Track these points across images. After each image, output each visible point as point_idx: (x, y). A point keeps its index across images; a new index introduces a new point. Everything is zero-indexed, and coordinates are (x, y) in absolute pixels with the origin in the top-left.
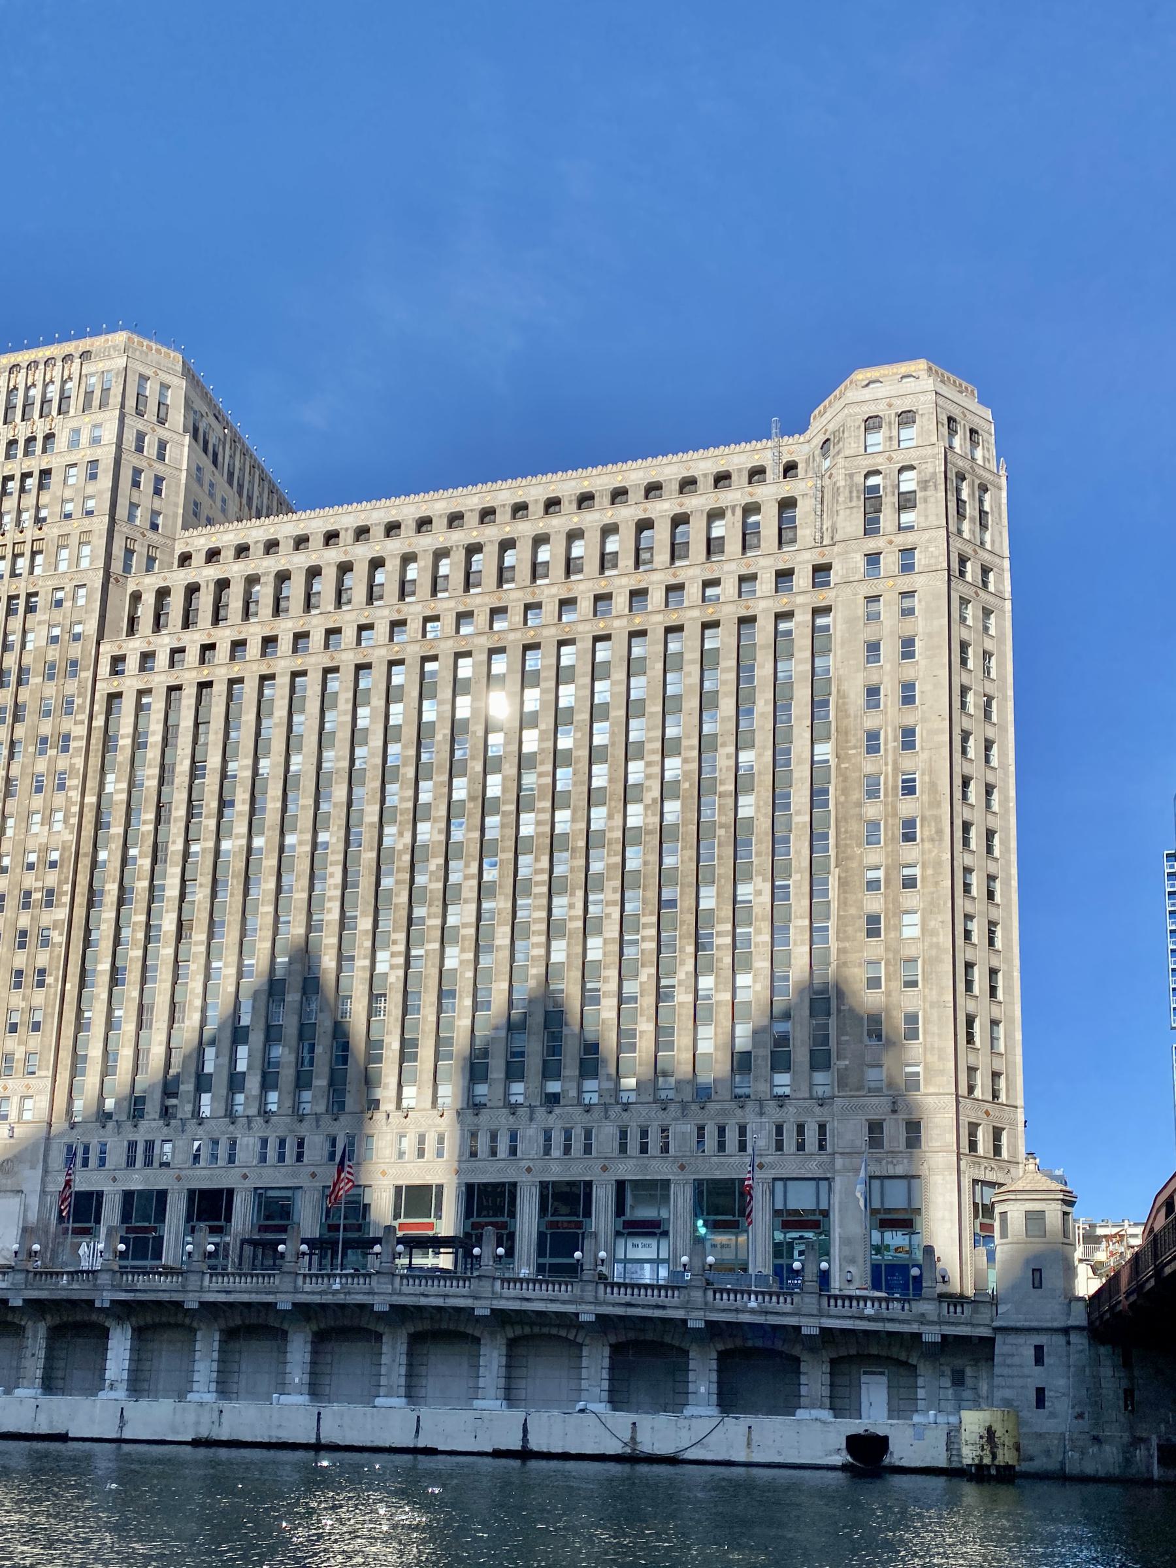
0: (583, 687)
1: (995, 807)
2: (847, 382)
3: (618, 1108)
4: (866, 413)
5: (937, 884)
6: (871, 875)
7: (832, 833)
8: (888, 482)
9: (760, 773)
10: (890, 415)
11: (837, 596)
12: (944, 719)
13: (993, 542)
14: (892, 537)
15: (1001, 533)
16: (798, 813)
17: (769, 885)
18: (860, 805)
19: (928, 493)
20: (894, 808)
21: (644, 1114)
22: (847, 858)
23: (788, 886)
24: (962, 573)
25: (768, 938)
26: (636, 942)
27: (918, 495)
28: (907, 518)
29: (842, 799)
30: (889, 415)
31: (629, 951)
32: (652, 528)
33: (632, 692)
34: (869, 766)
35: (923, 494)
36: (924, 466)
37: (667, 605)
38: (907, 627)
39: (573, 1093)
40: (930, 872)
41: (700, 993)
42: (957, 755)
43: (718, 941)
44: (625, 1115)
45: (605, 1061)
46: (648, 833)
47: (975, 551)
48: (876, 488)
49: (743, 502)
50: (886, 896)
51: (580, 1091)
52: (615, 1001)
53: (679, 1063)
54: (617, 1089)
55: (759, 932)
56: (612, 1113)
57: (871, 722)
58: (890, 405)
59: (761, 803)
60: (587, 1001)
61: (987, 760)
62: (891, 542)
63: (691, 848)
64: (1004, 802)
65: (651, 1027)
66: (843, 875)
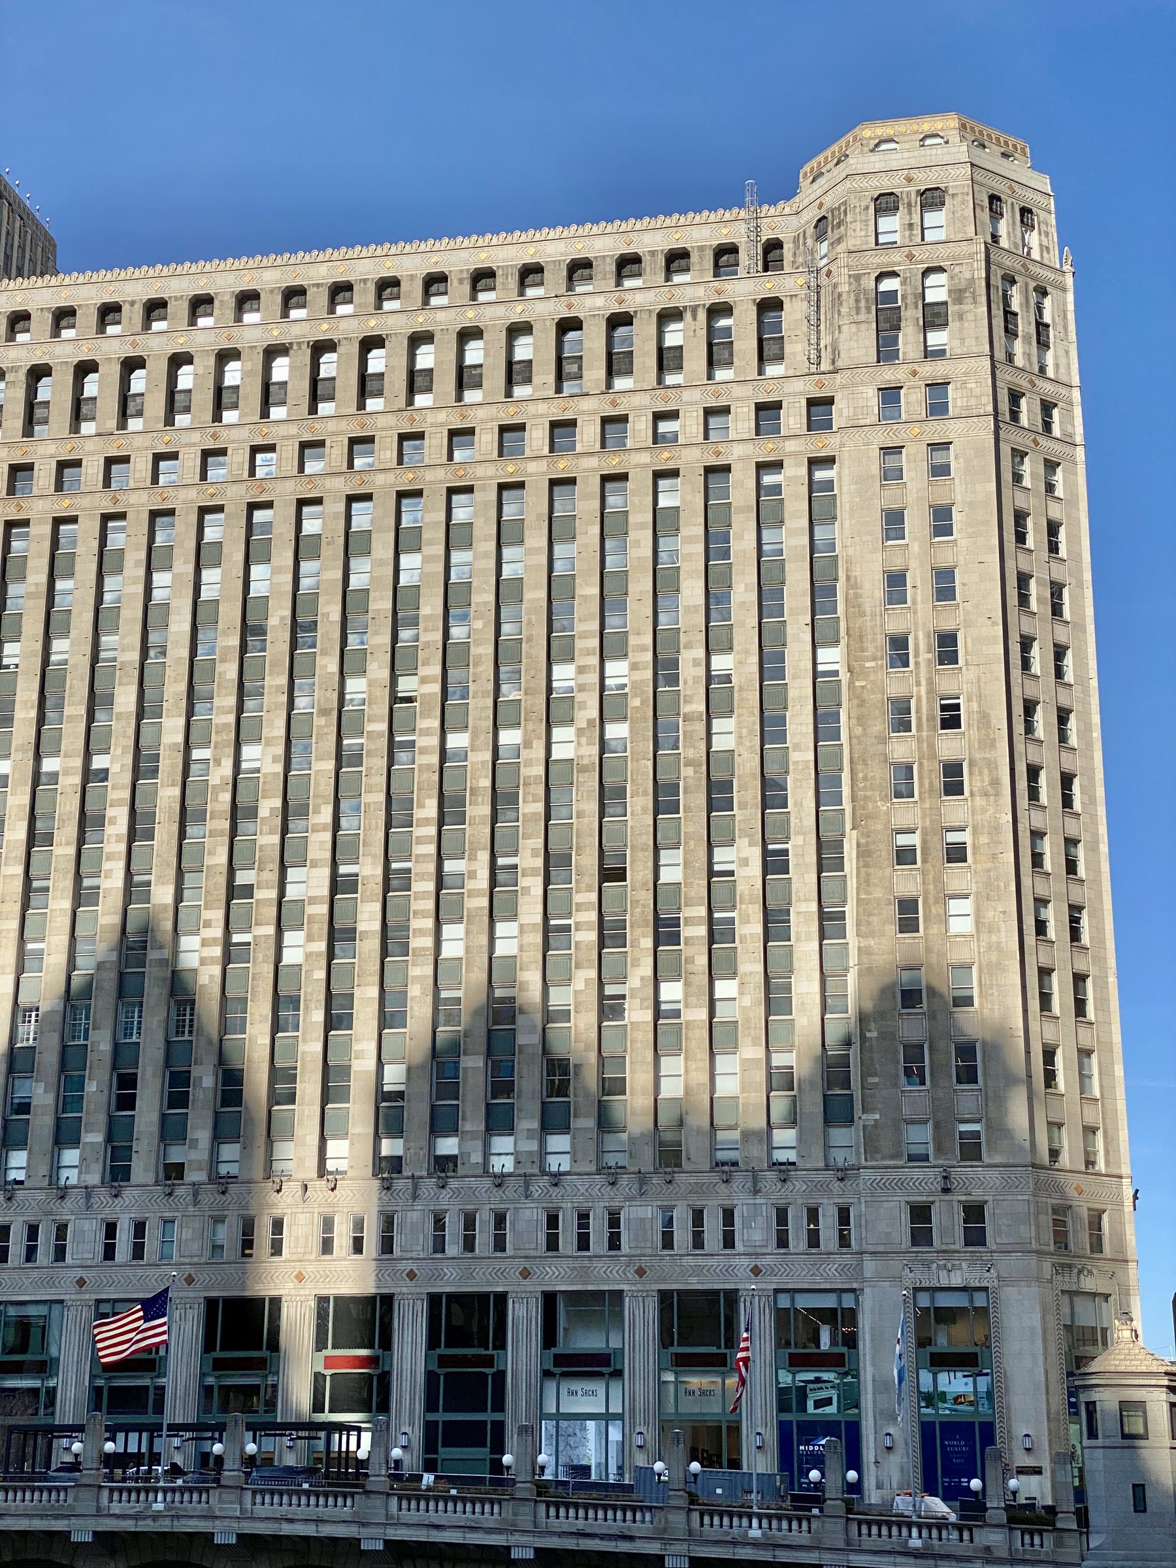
5: (994, 856)
6: (903, 840)
18: (883, 740)
29: (858, 731)
32: (581, 329)
37: (603, 446)
50: (924, 873)
66: (863, 841)
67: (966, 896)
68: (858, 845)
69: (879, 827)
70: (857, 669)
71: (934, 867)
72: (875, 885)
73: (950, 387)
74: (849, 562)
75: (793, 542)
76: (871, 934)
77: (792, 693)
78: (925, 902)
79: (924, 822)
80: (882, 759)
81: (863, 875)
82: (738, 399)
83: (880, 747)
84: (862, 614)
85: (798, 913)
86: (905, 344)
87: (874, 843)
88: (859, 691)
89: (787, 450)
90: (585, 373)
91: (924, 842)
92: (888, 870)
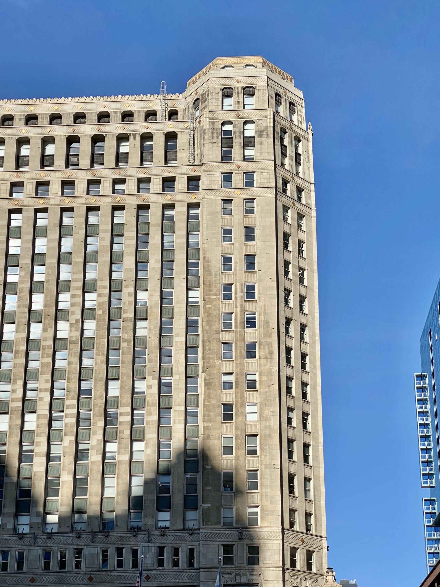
0: (27, 241)
1: (307, 339)
2: (211, 64)
3: (44, 537)
4: (223, 85)
6: (226, 378)
7: (200, 349)
8: (237, 130)
9: (151, 307)
10: (238, 88)
11: (204, 197)
12: (273, 281)
13: (304, 173)
14: (239, 164)
15: (309, 168)
16: (178, 335)
17: (157, 382)
18: (219, 332)
19: (263, 139)
20: (241, 335)
21: (63, 540)
22: (210, 367)
23: (170, 384)
24: (285, 191)
25: (156, 418)
26: (61, 418)
27: (257, 139)
28: (249, 153)
29: (207, 327)
30: (238, 88)
31: (56, 424)
32: (78, 142)
33: (63, 247)
34: (225, 307)
35: (259, 138)
36: (260, 122)
37: (88, 193)
38: (250, 221)
39: (10, 525)
40: (264, 378)
41: (107, 455)
42: (282, 304)
43: (120, 419)
44: (49, 542)
45: (36, 503)
46: (72, 342)
47: (292, 177)
48: (229, 132)
49: (141, 133)
51: (16, 524)
52: (44, 459)
53: (90, 504)
54: (44, 523)
55: (150, 414)
56: (39, 541)
57: (226, 279)
58: (238, 82)
59: (152, 327)
60: (23, 460)
61: (301, 309)
62: (239, 167)
63: (103, 354)
64: (312, 336)
65: (71, 478)
66: (207, 378)
67: (255, 404)
68: (205, 380)
69: (215, 372)
70: (207, 299)
71: (241, 390)
72: (213, 398)
73: (255, 174)
74: (205, 250)
75: (179, 241)
76: (210, 421)
77: (176, 310)
78: (236, 406)
79: (237, 370)
80: (218, 341)
81: (207, 393)
82: (154, 175)
83: (217, 335)
84: (211, 274)
85: (175, 411)
86: (235, 154)
87: (213, 379)
88: (208, 309)
89: (177, 199)
90: (80, 162)
91: (237, 379)
92: (220, 391)
